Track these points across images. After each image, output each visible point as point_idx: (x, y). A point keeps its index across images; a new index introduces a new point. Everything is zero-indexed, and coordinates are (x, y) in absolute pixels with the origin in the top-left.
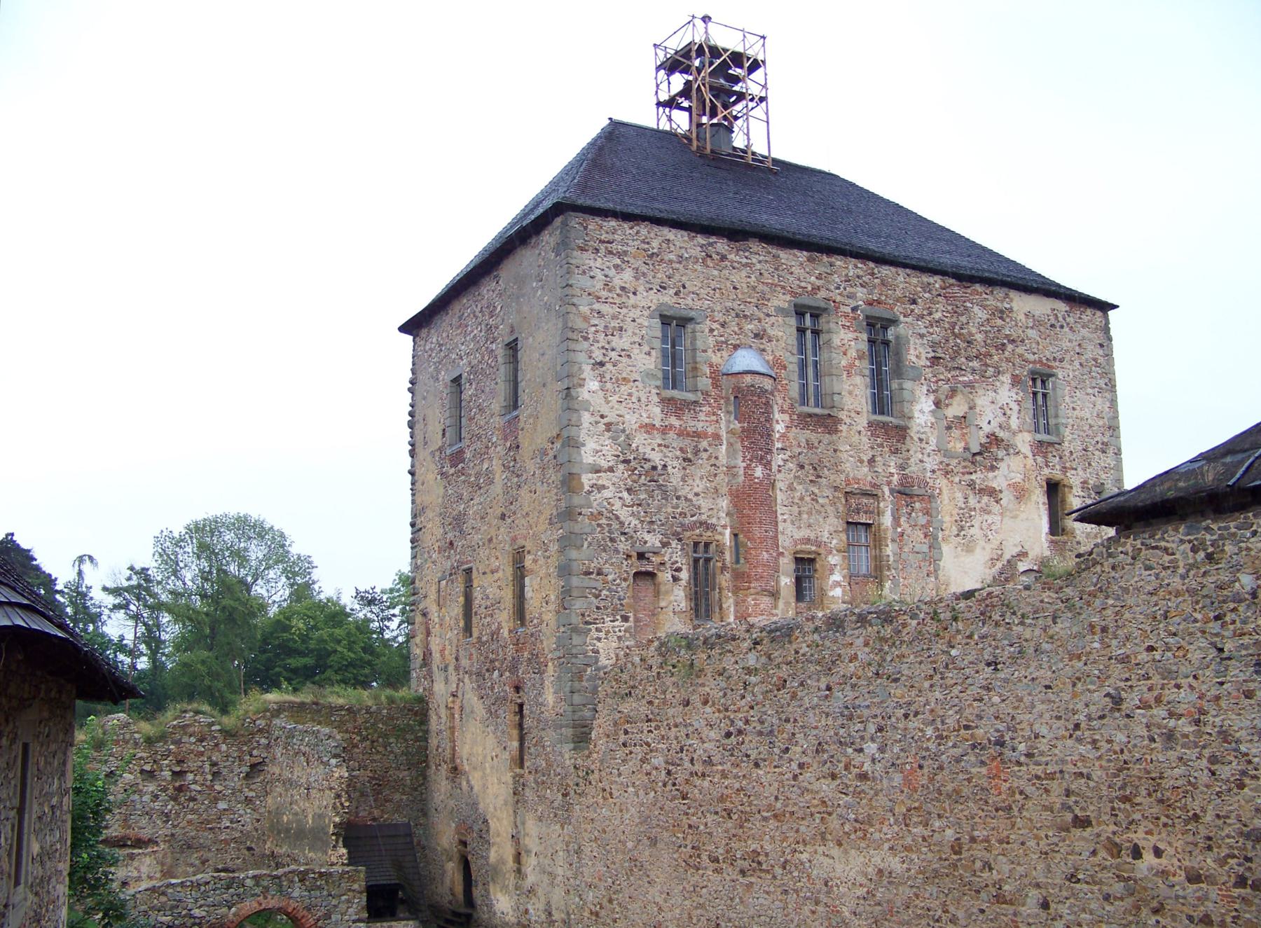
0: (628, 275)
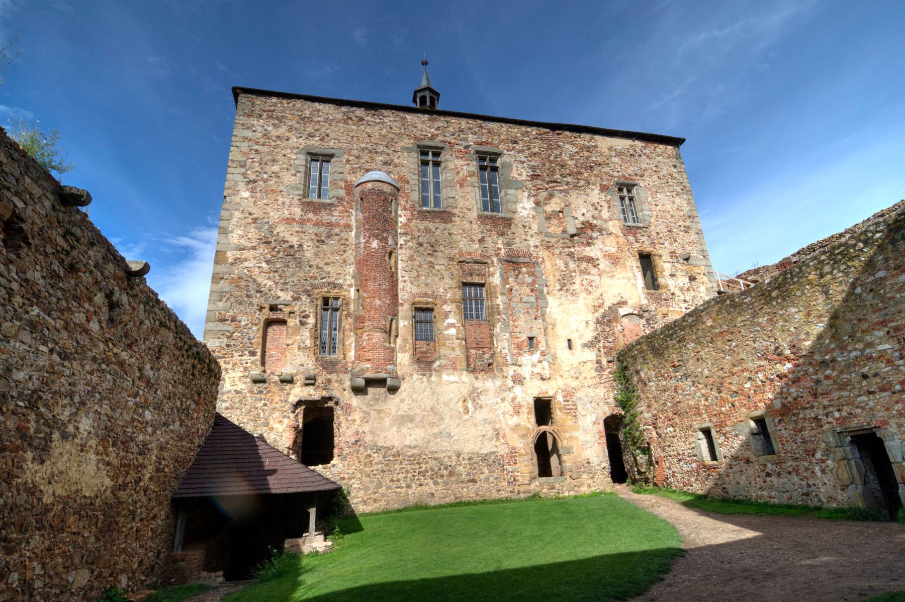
0: (282, 130)
